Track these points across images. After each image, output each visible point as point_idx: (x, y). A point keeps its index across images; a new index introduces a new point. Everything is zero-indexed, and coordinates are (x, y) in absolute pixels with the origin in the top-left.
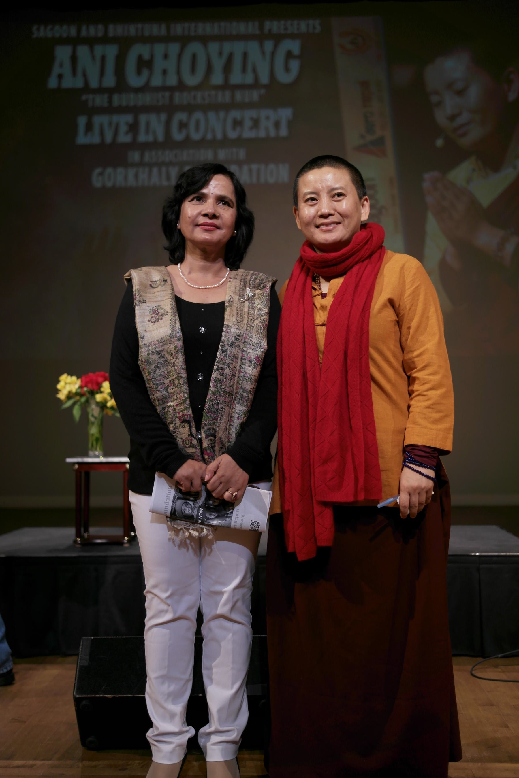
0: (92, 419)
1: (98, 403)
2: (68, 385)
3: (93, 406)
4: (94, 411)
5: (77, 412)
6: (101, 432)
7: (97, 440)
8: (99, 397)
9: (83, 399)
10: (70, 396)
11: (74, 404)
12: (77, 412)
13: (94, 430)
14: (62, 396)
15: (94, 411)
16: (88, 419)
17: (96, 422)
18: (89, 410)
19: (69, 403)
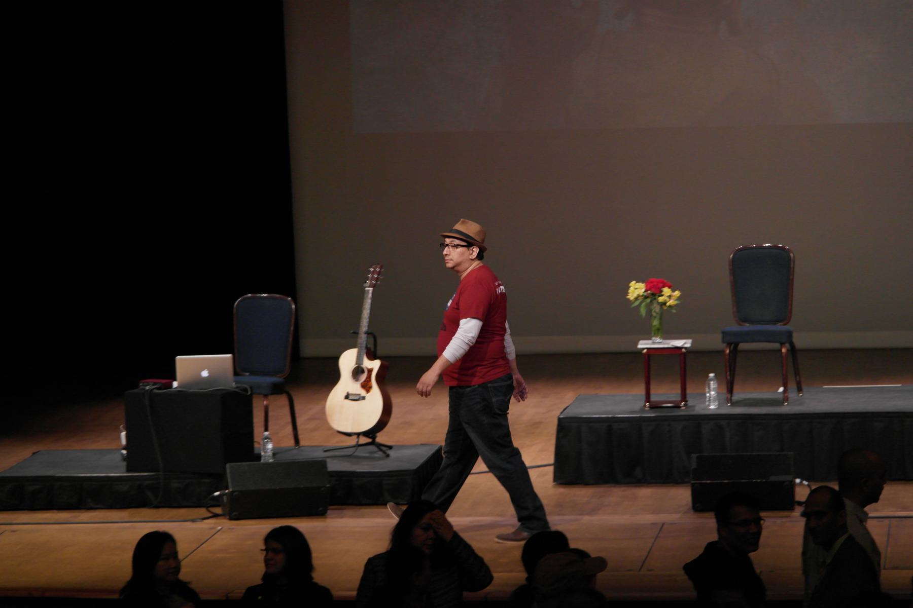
0: (654, 314)
1: (659, 303)
2: (637, 289)
3: (655, 305)
4: (656, 308)
5: (643, 311)
6: (661, 324)
7: (658, 330)
8: (661, 299)
9: (648, 300)
10: (636, 299)
11: (640, 304)
12: (643, 311)
13: (656, 323)
14: (632, 296)
15: (656, 308)
16: (651, 315)
17: (658, 317)
18: (652, 307)
19: (637, 303)
